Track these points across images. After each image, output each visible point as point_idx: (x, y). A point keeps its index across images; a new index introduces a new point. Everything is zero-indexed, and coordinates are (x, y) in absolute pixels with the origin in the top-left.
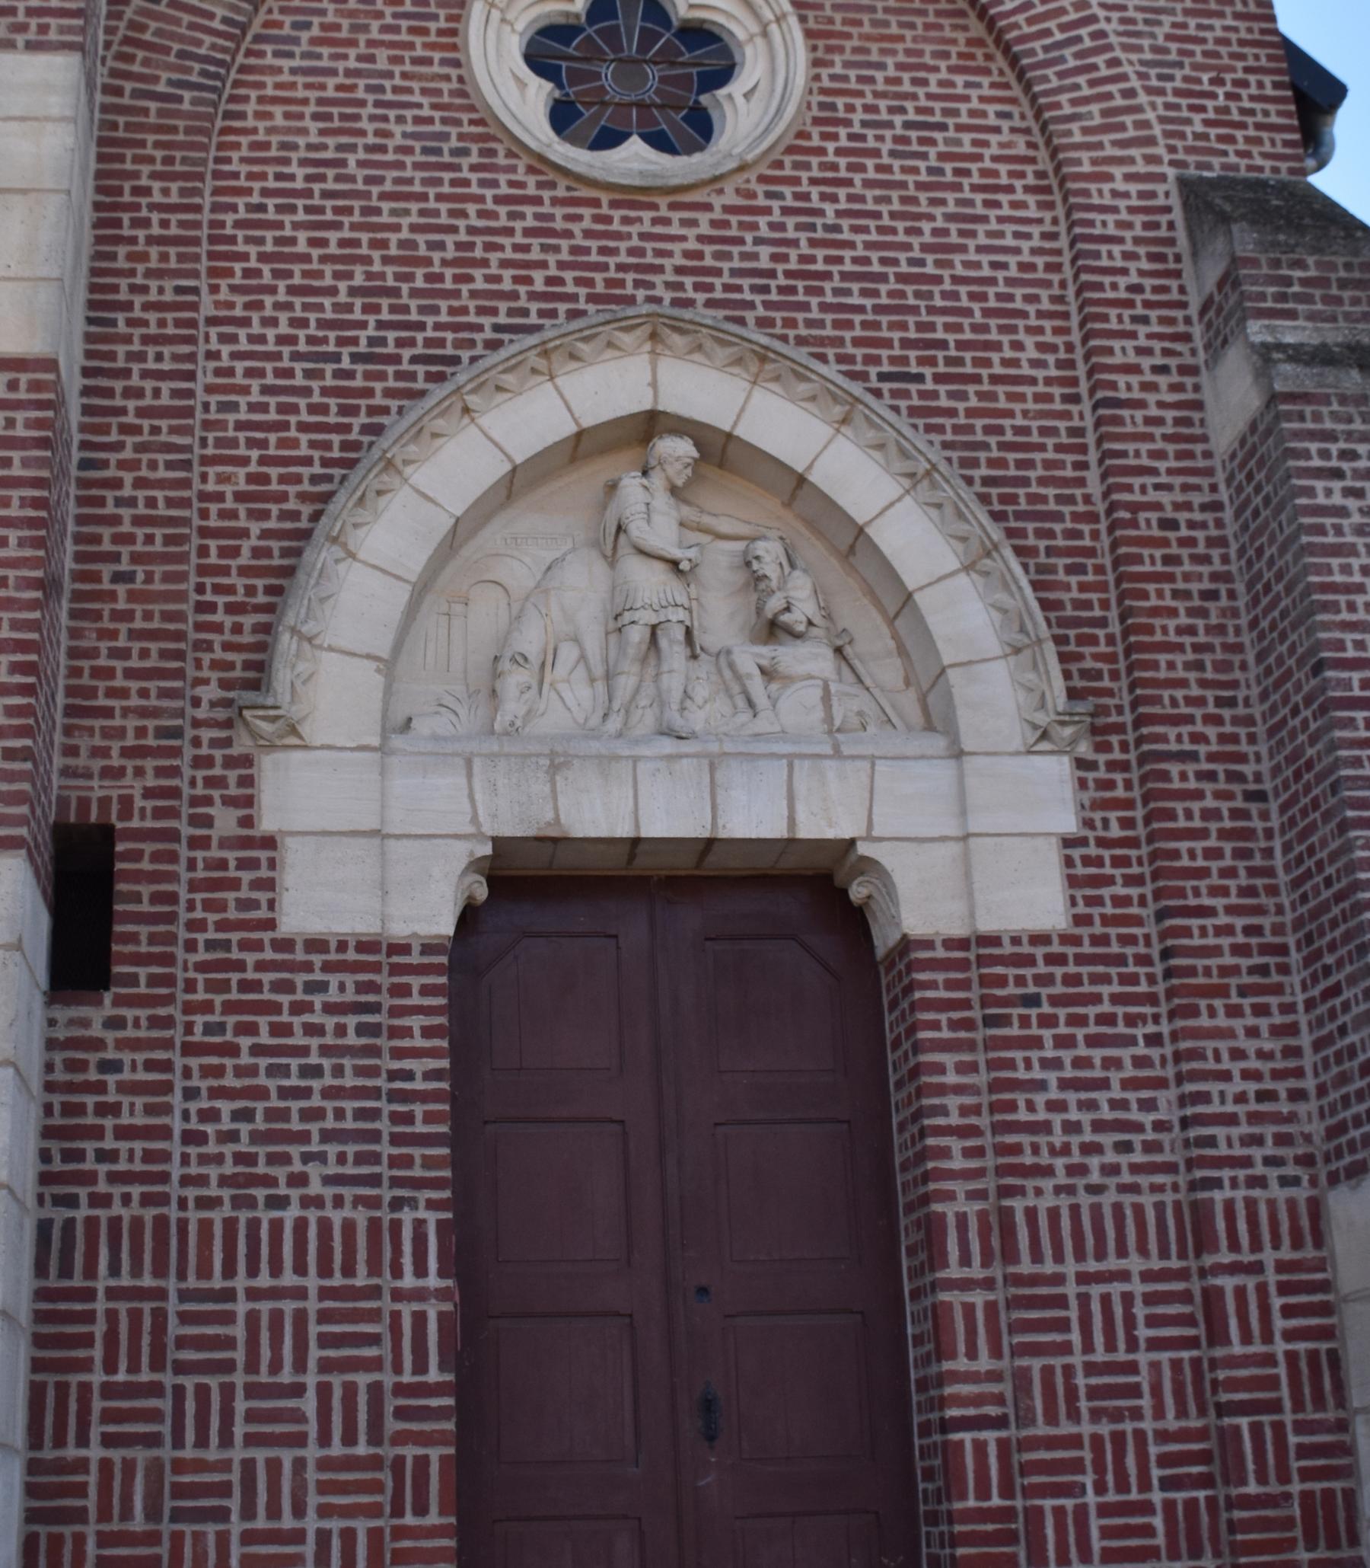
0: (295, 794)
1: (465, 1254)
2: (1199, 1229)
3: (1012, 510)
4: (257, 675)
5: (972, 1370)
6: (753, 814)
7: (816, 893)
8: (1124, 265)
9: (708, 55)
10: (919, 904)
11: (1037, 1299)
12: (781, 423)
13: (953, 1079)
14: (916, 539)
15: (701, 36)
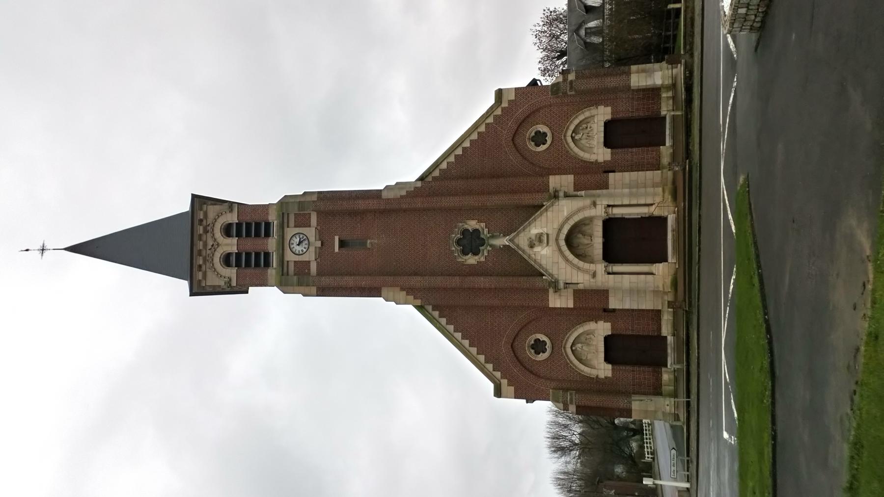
0: (601, 159)
1: (632, 147)
2: (633, 98)
3: (579, 109)
4: (592, 163)
5: (641, 114)
6: (602, 129)
7: (607, 124)
8: (558, 100)
9: (538, 133)
10: (609, 117)
11: (637, 110)
12: (572, 127)
13: (621, 116)
14: (581, 117)
15: (536, 133)
